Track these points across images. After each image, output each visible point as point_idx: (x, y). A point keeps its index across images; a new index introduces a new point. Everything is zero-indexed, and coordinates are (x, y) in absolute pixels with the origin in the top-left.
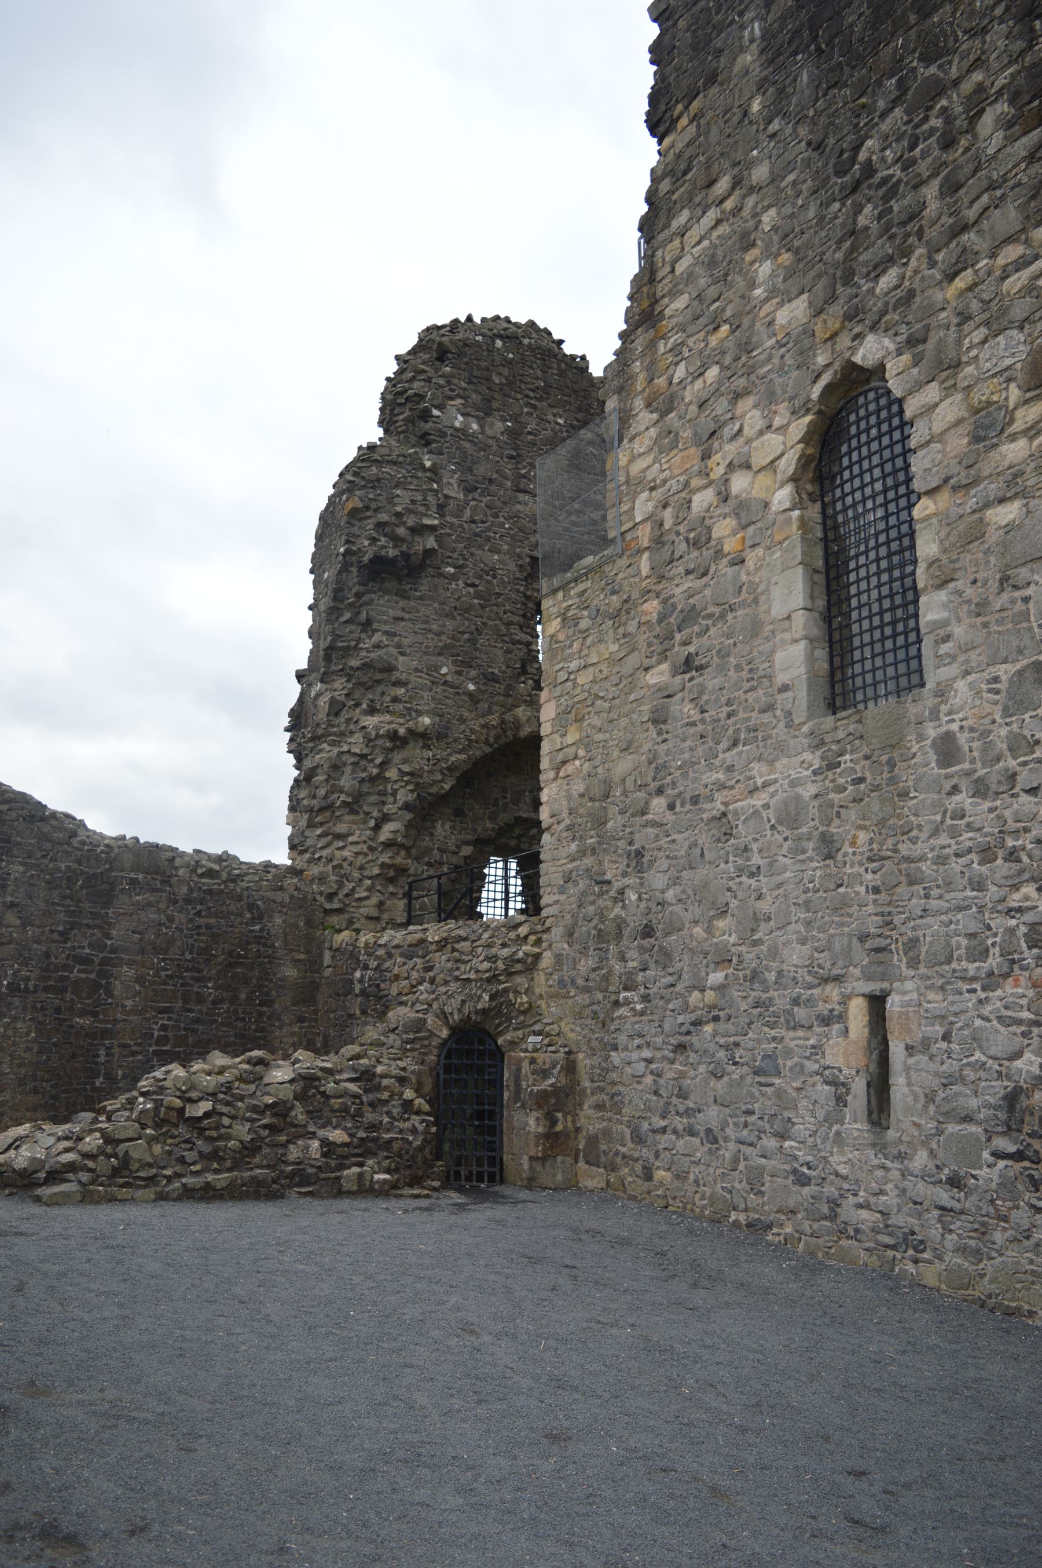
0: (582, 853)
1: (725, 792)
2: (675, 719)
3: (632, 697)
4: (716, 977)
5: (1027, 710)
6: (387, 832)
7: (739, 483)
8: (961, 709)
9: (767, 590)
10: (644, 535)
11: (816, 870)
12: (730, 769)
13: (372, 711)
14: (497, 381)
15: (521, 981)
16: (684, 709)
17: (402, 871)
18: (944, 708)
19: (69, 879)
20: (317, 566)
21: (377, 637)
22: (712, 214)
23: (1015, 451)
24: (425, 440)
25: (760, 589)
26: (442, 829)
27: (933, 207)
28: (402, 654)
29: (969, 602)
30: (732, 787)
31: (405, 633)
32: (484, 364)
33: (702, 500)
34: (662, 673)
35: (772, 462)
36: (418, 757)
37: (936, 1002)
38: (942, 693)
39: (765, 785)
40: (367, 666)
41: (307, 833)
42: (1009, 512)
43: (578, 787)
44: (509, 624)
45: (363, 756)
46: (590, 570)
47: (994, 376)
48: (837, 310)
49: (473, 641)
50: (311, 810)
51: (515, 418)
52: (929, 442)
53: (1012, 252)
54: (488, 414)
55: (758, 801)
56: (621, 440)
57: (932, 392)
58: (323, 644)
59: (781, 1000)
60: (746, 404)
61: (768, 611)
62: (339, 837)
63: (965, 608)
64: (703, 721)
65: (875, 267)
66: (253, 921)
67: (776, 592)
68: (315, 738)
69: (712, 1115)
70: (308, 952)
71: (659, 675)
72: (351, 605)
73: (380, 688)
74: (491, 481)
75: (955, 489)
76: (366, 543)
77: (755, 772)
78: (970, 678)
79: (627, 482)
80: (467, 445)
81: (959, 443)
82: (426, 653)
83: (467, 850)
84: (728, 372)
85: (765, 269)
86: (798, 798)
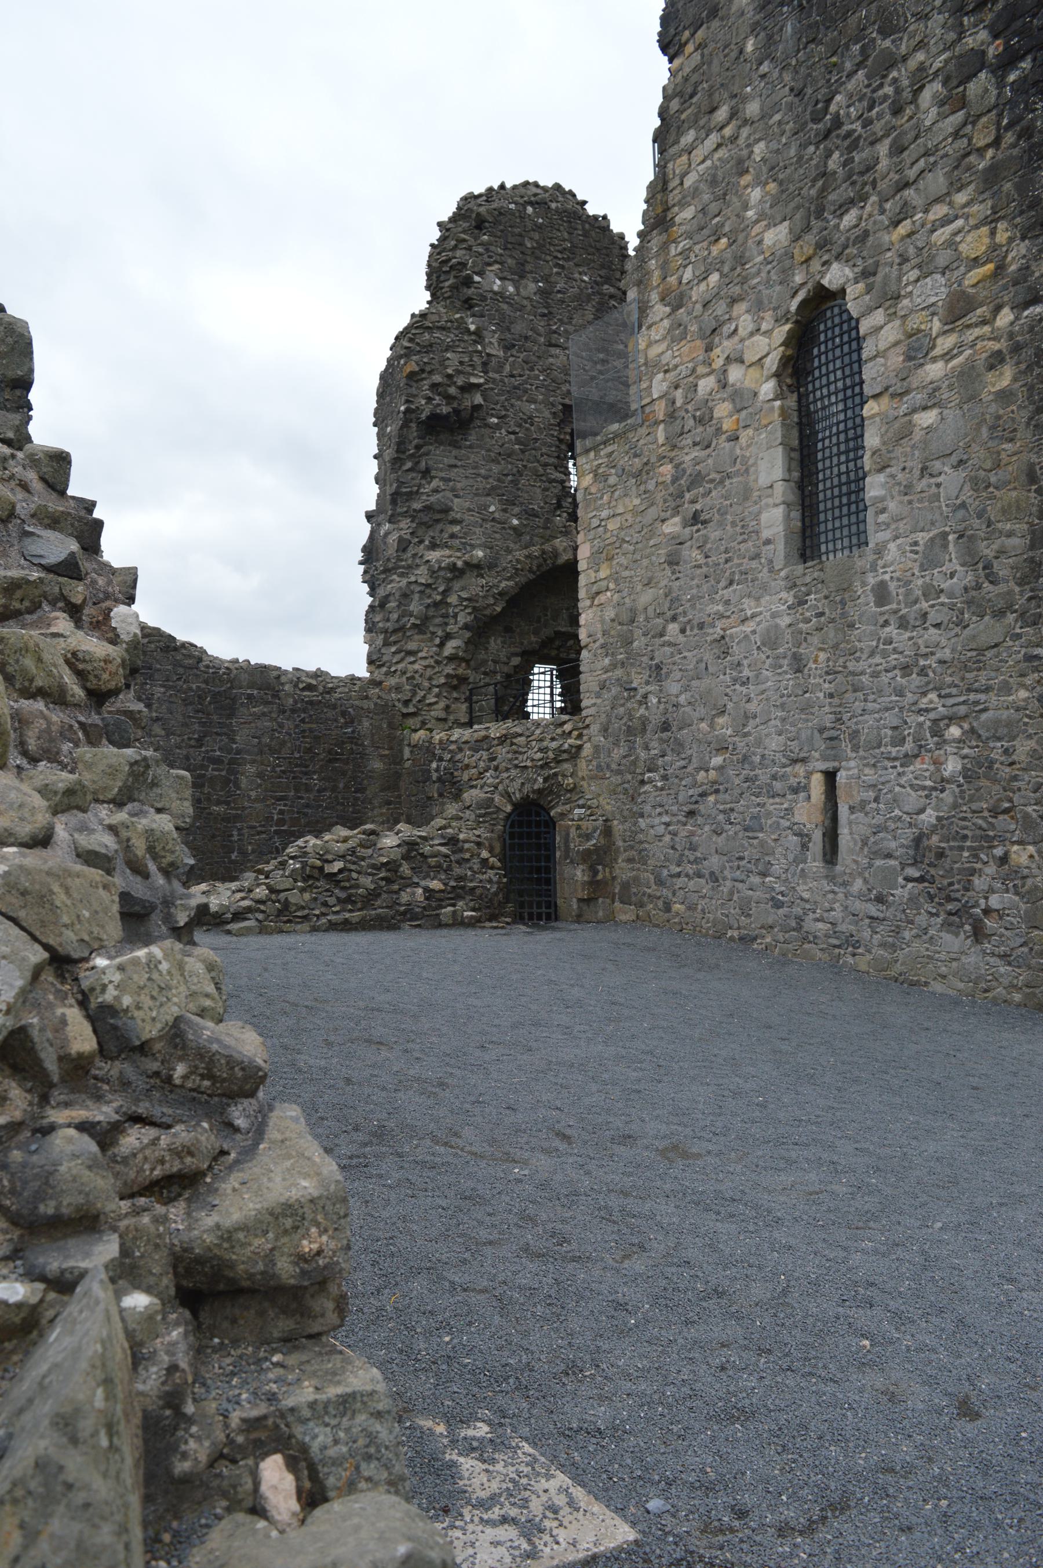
0: (614, 666)
1: (724, 621)
2: (685, 562)
3: (652, 543)
4: (717, 760)
5: (936, 567)
6: (449, 648)
7: (735, 374)
8: (892, 564)
9: (755, 464)
10: (660, 410)
11: (789, 680)
12: (727, 603)
13: (433, 546)
14: (529, 245)
15: (567, 766)
16: (692, 554)
17: (463, 680)
18: (880, 563)
19: (199, 697)
20: (380, 419)
21: (435, 483)
22: (714, 138)
23: (935, 370)
24: (468, 304)
25: (751, 462)
26: (495, 644)
27: (884, 163)
28: (456, 496)
29: (899, 484)
30: (729, 617)
31: (459, 479)
32: (517, 230)
33: (706, 385)
34: (675, 525)
35: (760, 359)
36: (475, 585)
37: (870, 775)
38: (879, 552)
39: (753, 616)
40: (428, 508)
41: (383, 651)
42: (928, 418)
43: (610, 613)
44: (546, 465)
45: (428, 586)
46: (617, 436)
47: (923, 309)
48: (811, 238)
49: (515, 483)
50: (386, 632)
51: (546, 279)
52: (876, 356)
53: (939, 211)
54: (522, 277)
55: (748, 628)
56: (640, 327)
57: (878, 317)
58: (390, 490)
59: (763, 776)
60: (741, 308)
61: (756, 480)
62: (410, 653)
63: (897, 488)
64: (707, 564)
65: (840, 207)
66: (346, 725)
67: (763, 466)
68: (386, 571)
69: (714, 862)
70: (391, 748)
71: (673, 526)
72: (412, 455)
73: (439, 526)
74: (526, 338)
75: (893, 396)
76: (423, 402)
77: (745, 606)
78: (899, 541)
79: (646, 364)
80: (505, 306)
81: (896, 359)
82: (476, 495)
83: (516, 661)
84: (727, 279)
85: (755, 194)
86: (777, 626)
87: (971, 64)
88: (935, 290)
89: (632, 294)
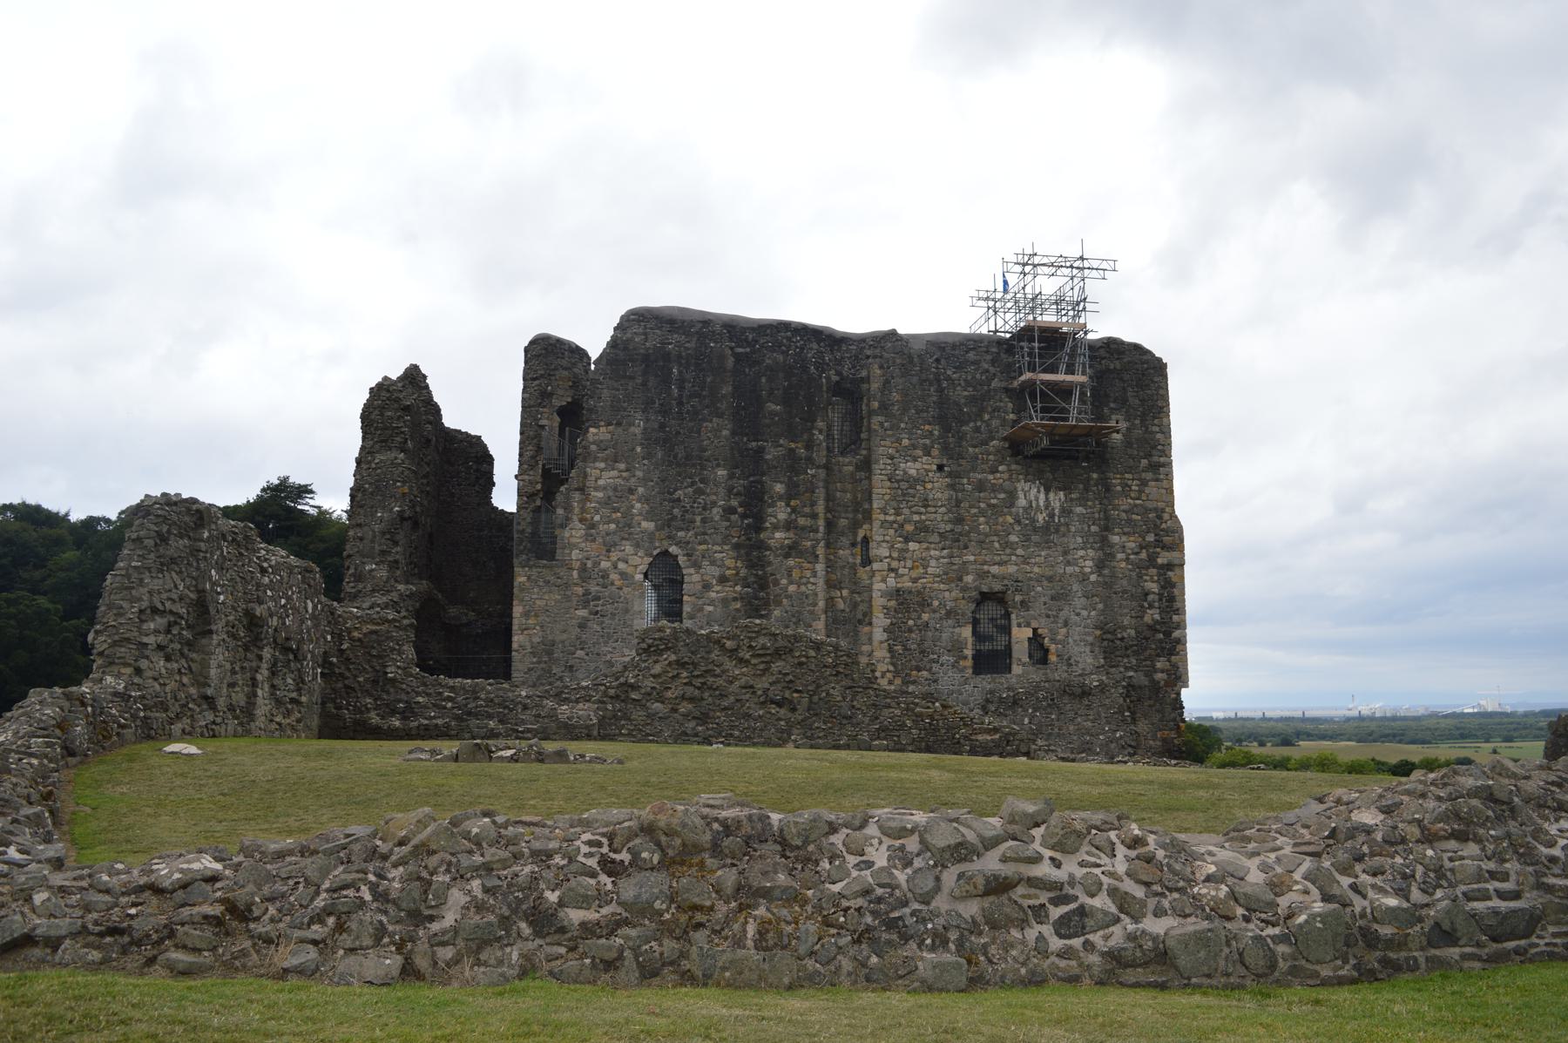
7: (621, 565)
10: (576, 565)
42: (711, 608)
43: (536, 640)
57: (692, 571)
85: (638, 505)
87: (732, 511)
88: (716, 571)
89: (560, 511)
